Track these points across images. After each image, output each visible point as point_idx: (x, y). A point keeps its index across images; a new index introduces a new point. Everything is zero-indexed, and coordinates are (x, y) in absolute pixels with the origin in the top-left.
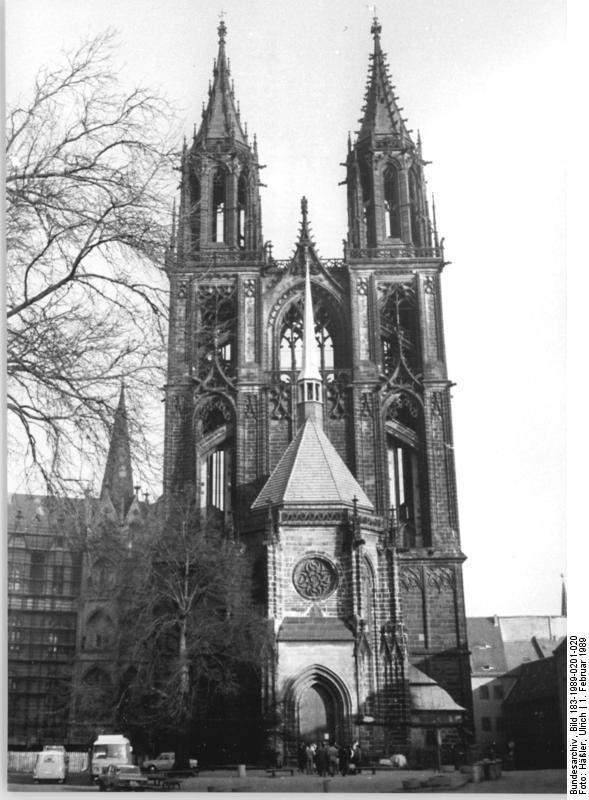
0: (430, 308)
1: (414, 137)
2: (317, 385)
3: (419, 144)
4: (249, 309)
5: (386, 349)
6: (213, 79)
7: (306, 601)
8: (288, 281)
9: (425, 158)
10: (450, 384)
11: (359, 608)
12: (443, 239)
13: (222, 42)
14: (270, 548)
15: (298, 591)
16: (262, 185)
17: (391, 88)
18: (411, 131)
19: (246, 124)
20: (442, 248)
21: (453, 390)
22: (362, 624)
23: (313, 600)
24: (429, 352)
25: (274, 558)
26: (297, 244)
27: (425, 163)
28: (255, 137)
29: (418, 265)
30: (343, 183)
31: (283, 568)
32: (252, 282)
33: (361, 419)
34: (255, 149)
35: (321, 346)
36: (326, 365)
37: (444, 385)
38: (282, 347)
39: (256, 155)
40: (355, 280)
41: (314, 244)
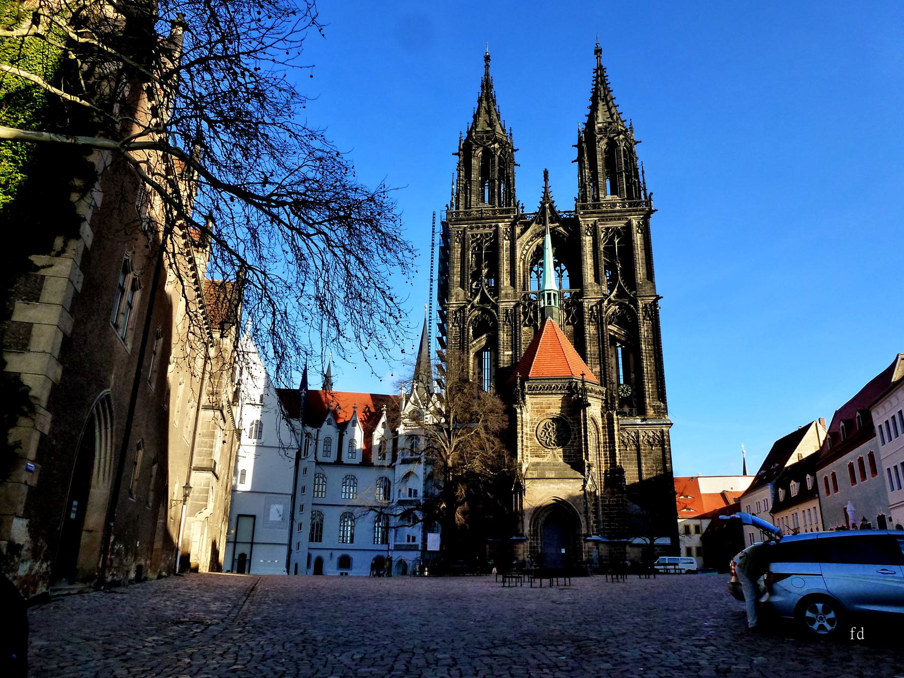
0: (641, 244)
4: (507, 248)
7: (546, 450)
10: (658, 298)
11: (587, 455)
12: (651, 194)
13: (487, 66)
14: (519, 411)
16: (517, 165)
20: (650, 200)
22: (589, 466)
25: (522, 418)
26: (541, 202)
29: (633, 213)
31: (528, 425)
37: (654, 298)
40: (584, 226)
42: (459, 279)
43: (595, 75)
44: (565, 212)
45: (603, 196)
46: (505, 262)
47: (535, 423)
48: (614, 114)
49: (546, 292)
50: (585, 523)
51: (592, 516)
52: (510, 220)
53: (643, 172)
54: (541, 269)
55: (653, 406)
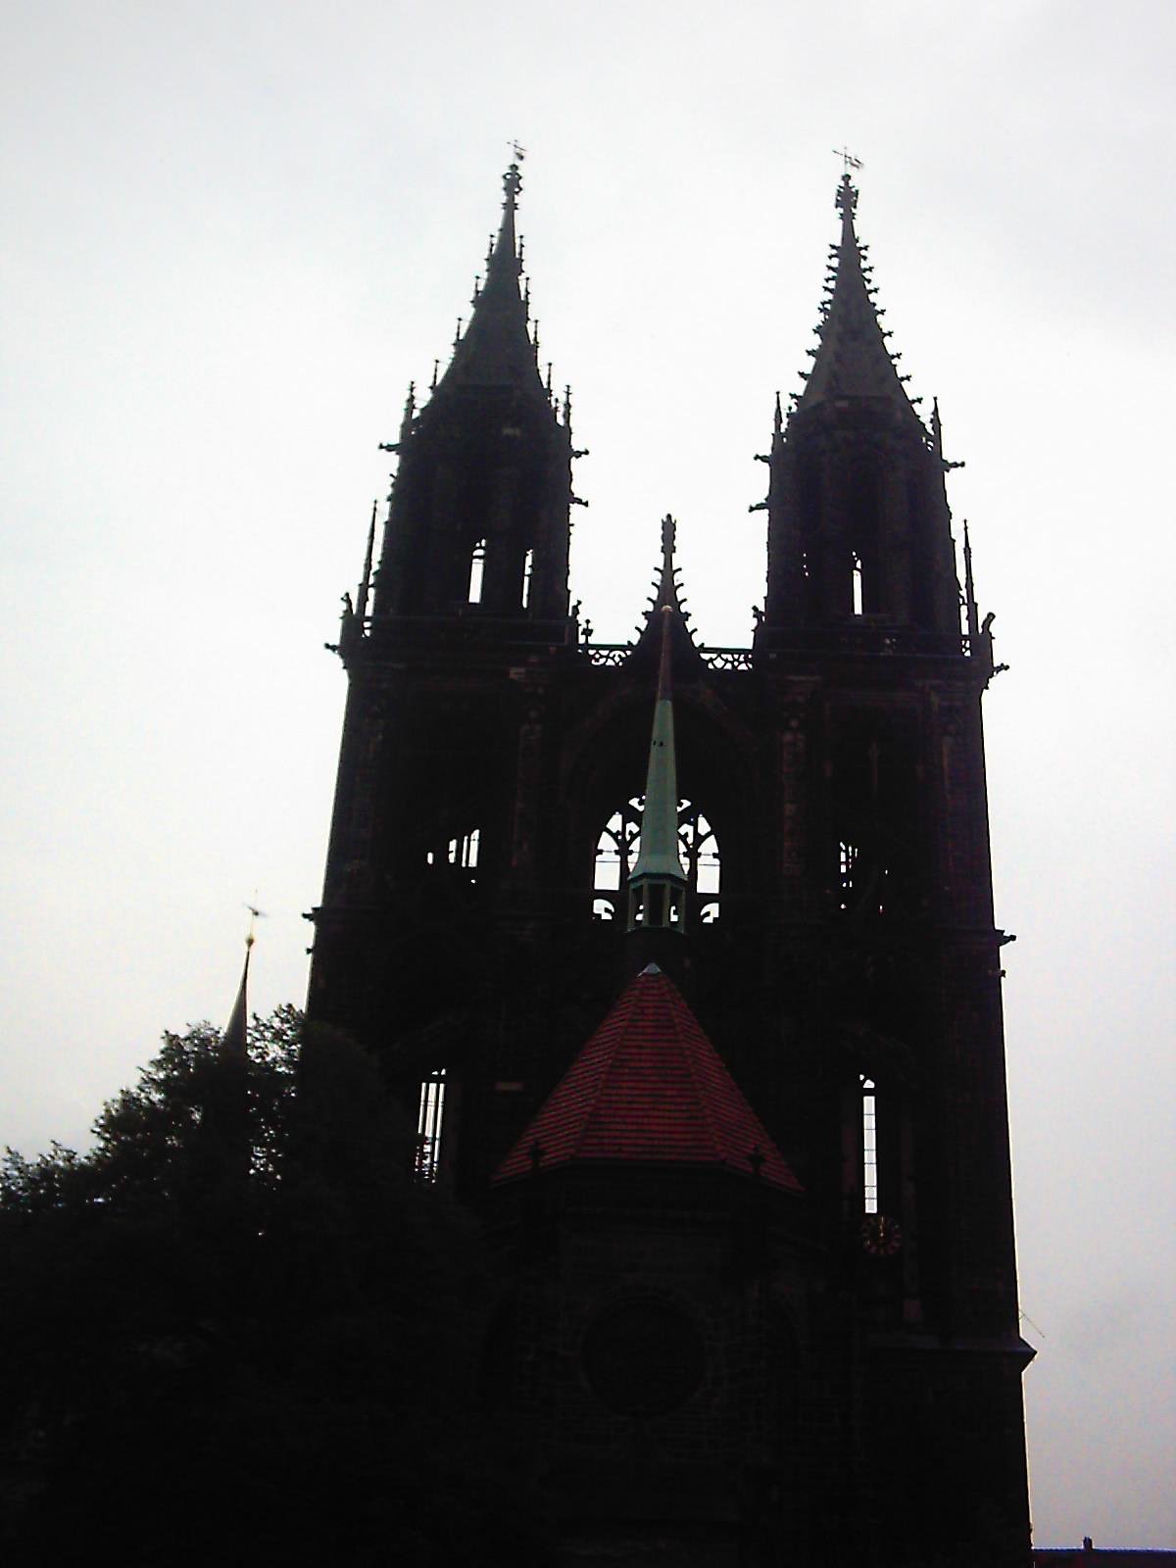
1: (924, 412)
3: (936, 421)
5: (843, 858)
6: (485, 275)
9: (948, 455)
10: (1003, 939)
12: (991, 616)
13: (510, 207)
16: (580, 501)
18: (919, 400)
28: (568, 394)
34: (567, 416)
38: (601, 852)
39: (567, 431)
43: (835, 263)
44: (720, 651)
49: (644, 882)
53: (967, 551)
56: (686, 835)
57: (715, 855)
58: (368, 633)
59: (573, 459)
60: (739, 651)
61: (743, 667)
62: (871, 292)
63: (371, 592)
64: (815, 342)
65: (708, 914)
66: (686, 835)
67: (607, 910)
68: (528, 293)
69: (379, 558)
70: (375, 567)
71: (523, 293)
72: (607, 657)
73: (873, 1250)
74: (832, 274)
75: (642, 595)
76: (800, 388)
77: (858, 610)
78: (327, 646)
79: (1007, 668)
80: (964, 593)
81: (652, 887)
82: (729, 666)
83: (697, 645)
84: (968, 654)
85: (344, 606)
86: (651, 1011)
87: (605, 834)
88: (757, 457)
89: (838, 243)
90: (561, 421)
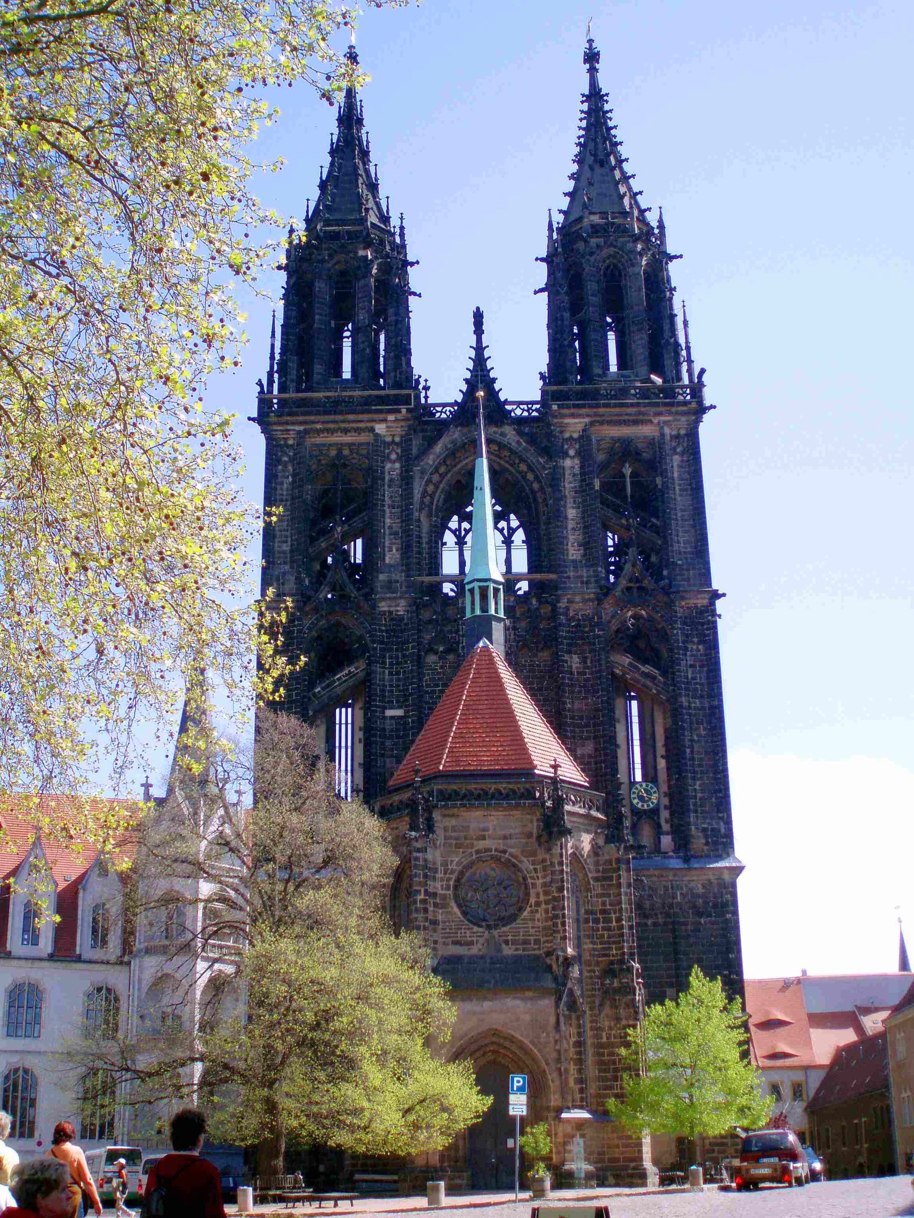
0: (681, 479)
1: (652, 218)
2: (496, 591)
3: (661, 226)
5: (610, 543)
6: (336, 131)
7: (476, 929)
8: (455, 434)
9: (671, 249)
10: (716, 595)
12: (703, 371)
15: (465, 914)
16: (414, 294)
17: (617, 144)
18: (649, 209)
19: (388, 198)
20: (701, 385)
21: (720, 605)
23: (489, 927)
24: (681, 541)
26: (466, 380)
27: (672, 258)
28: (402, 219)
30: (541, 290)
32: (397, 439)
33: (570, 652)
34: (402, 235)
35: (508, 542)
36: (515, 570)
37: (707, 596)
39: (403, 246)
41: (494, 380)
42: (286, 547)
43: (585, 107)
44: (519, 403)
45: (600, 371)
46: (387, 511)
47: (452, 872)
48: (625, 194)
49: (476, 585)
50: (557, 1083)
51: (572, 1068)
52: (399, 416)
53: (686, 323)
54: (465, 525)
55: (704, 830)
56: (503, 529)
57: (523, 542)
58: (276, 406)
59: (409, 267)
60: (533, 403)
61: (535, 414)
62: (612, 128)
63: (276, 376)
64: (575, 168)
65: (520, 589)
66: (503, 529)
67: (452, 590)
68: (368, 142)
69: (279, 351)
70: (277, 357)
71: (365, 143)
72: (441, 412)
73: (640, 805)
74: (583, 115)
75: (462, 368)
76: (565, 203)
77: (613, 368)
78: (249, 419)
79: (715, 407)
80: (684, 353)
81: (480, 587)
82: (526, 414)
83: (502, 399)
84: (688, 397)
85: (258, 389)
86: (485, 671)
87: (447, 532)
88: (537, 259)
89: (587, 93)
90: (398, 240)
